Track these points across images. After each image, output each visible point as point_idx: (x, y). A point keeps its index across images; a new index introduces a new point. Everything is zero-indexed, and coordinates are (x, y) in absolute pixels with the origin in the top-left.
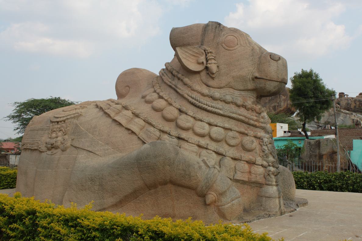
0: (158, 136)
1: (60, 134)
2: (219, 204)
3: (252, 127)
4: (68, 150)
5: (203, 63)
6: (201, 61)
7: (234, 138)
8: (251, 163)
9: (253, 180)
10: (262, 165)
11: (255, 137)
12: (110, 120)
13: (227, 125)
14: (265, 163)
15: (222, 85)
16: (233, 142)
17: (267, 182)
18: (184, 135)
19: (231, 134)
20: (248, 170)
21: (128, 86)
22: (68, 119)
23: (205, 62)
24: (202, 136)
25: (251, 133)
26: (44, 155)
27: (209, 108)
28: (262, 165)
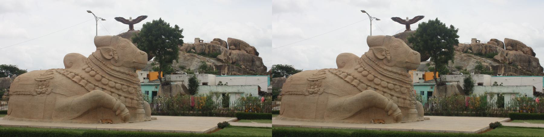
0: (94, 87)
1: (44, 87)
2: (121, 115)
3: (132, 84)
4: (51, 95)
5: (111, 55)
6: (110, 54)
7: (125, 88)
8: (132, 99)
9: (133, 106)
10: (137, 100)
11: (134, 88)
12: (71, 81)
13: (122, 83)
14: (138, 99)
15: (120, 65)
16: (125, 90)
17: (139, 107)
18: (104, 87)
19: (124, 86)
20: (131, 102)
21: (72, 62)
22: (47, 80)
23: (112, 54)
24: (112, 87)
25: (132, 86)
26: (36, 97)
27: (115, 76)
28: (137, 100)
